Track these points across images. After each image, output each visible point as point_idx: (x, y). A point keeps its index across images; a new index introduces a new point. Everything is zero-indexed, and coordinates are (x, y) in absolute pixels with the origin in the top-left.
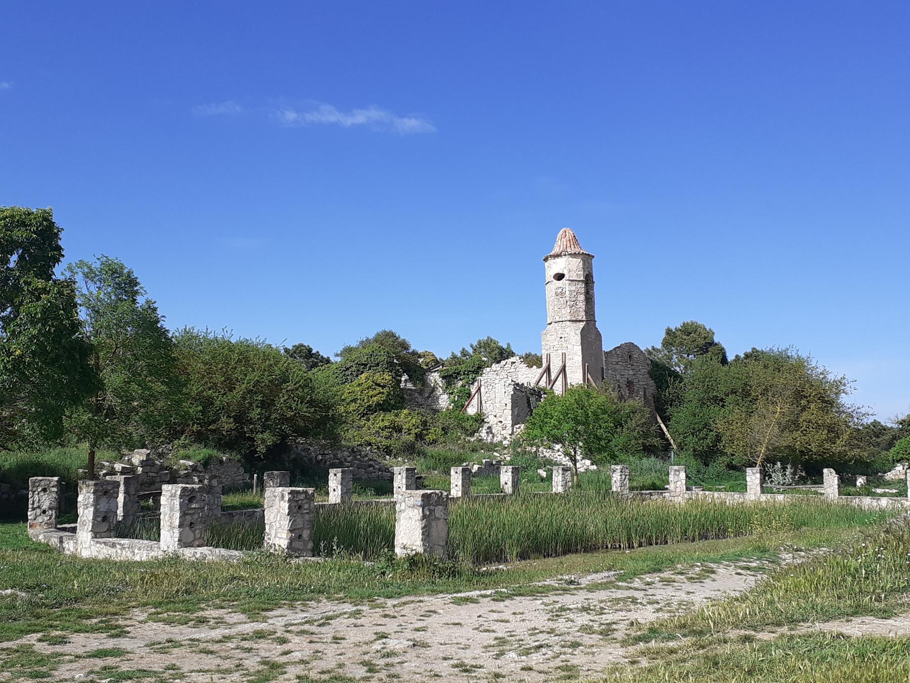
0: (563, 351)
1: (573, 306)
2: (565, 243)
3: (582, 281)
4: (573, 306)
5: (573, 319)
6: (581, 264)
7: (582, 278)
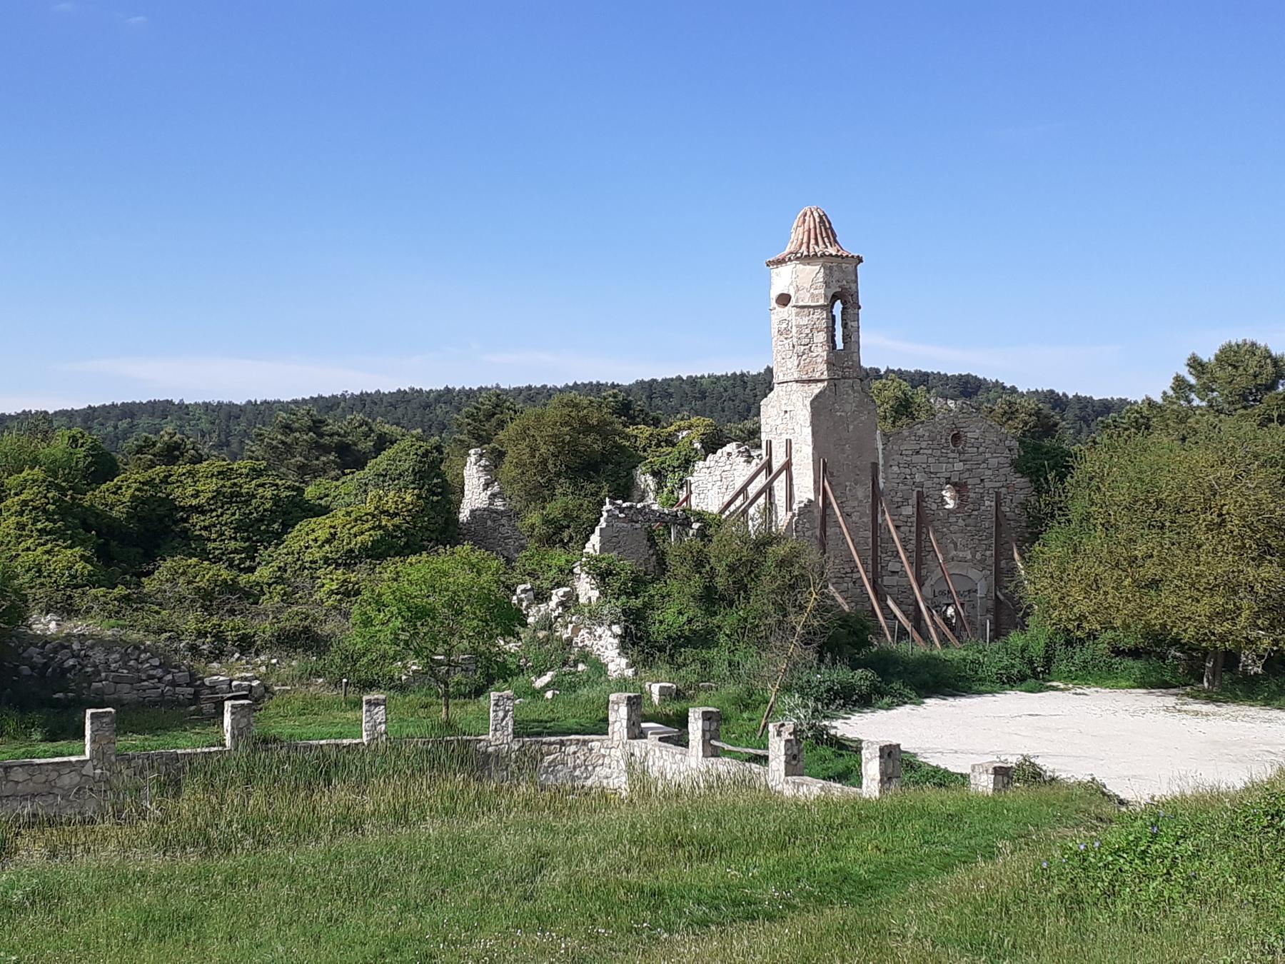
0: (789, 437)
1: (804, 353)
2: (800, 237)
3: (821, 307)
4: (804, 353)
5: (805, 377)
6: (821, 275)
7: (821, 302)
